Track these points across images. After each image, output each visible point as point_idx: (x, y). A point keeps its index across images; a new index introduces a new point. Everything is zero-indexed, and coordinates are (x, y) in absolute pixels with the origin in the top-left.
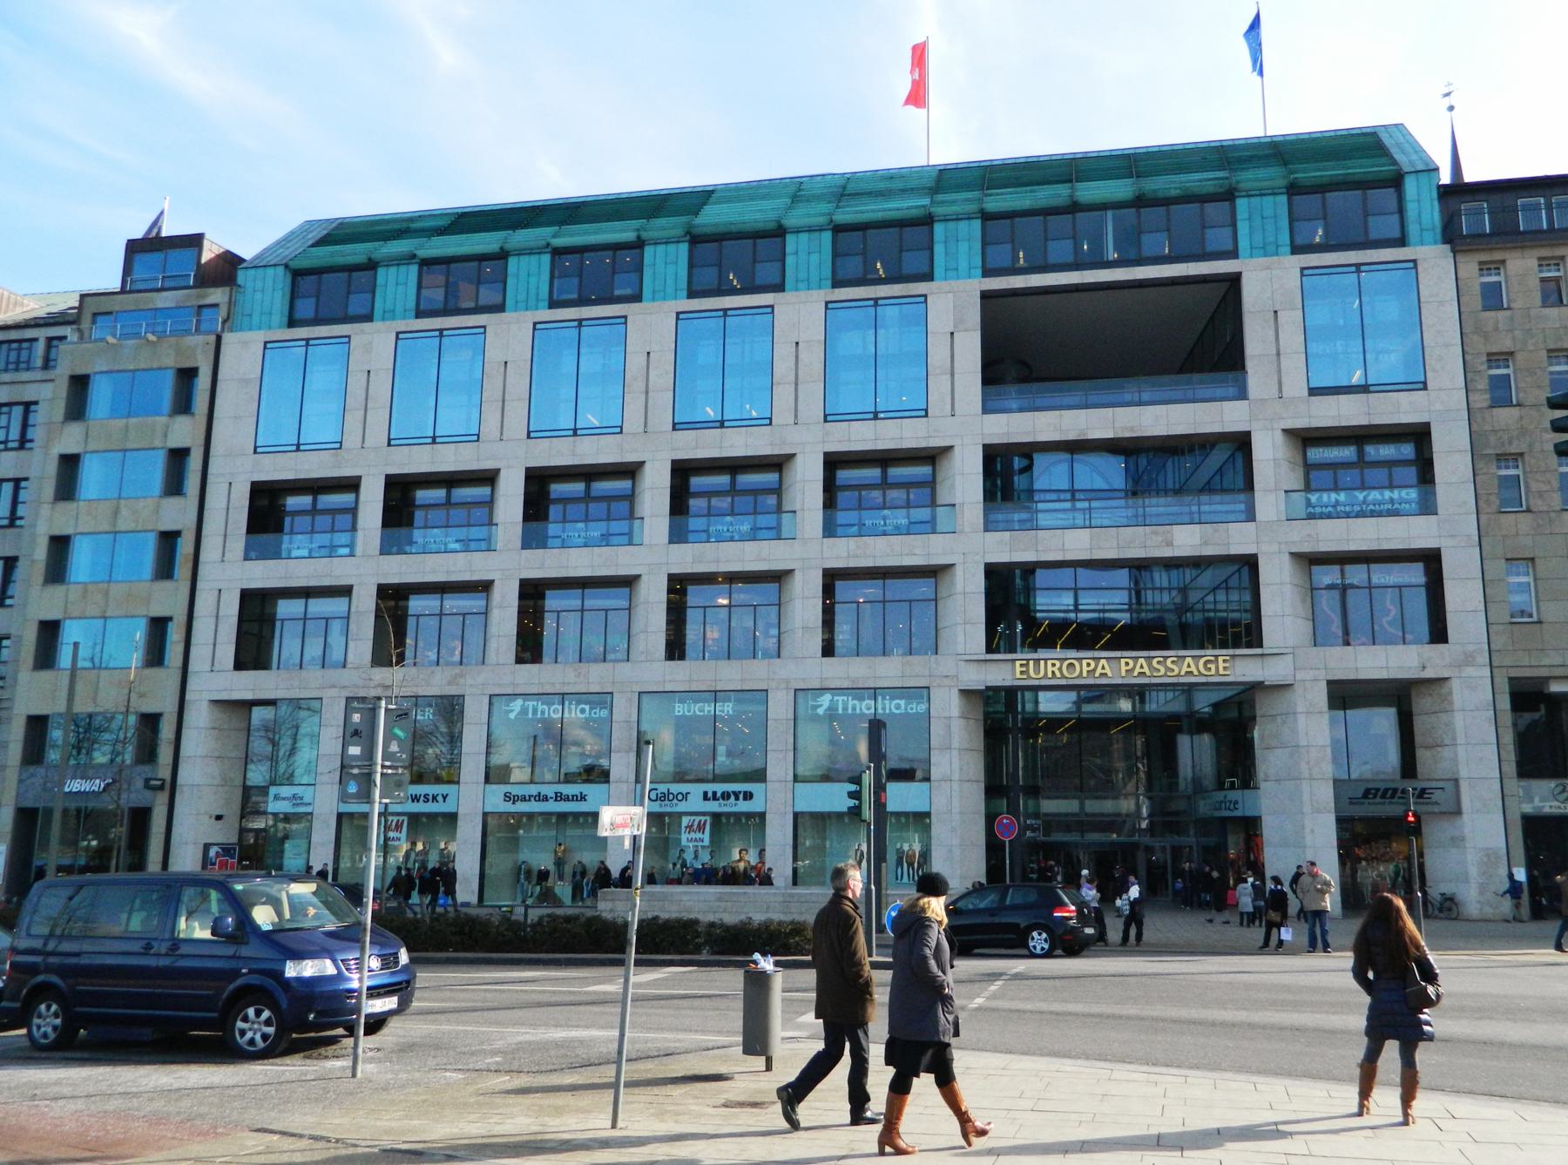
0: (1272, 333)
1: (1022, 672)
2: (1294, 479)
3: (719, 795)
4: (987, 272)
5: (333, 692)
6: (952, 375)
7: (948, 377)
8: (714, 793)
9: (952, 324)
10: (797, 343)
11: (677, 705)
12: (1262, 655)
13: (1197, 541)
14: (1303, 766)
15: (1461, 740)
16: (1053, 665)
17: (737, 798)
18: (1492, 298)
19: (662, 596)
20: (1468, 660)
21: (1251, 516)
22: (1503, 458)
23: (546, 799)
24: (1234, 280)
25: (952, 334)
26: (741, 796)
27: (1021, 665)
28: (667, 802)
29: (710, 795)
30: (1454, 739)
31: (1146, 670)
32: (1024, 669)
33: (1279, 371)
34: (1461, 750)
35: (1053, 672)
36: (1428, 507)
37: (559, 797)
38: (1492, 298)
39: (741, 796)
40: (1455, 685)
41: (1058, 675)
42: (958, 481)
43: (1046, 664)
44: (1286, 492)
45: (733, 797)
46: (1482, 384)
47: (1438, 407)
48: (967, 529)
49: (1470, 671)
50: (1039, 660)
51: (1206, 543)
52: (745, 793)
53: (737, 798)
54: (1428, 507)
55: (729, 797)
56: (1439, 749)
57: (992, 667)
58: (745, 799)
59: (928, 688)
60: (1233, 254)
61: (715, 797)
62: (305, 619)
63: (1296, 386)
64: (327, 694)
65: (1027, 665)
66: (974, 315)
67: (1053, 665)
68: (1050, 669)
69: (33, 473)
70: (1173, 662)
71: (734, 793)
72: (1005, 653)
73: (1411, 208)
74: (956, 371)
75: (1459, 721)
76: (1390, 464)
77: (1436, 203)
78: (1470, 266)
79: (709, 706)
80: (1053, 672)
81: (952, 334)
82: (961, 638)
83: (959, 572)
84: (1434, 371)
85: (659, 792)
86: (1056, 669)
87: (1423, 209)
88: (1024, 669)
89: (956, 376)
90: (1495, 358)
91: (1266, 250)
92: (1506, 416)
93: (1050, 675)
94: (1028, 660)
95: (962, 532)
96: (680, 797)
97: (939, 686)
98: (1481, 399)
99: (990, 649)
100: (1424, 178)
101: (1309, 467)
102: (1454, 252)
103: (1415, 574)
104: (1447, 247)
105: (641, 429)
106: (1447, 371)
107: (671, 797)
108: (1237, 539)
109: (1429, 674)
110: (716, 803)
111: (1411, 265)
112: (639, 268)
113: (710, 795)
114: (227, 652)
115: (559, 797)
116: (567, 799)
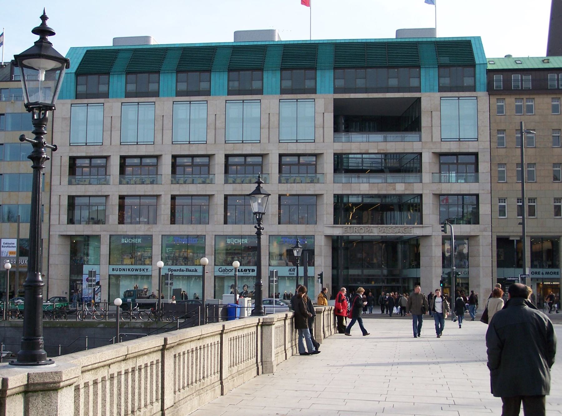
0: (430, 119)
1: (345, 231)
3: (243, 270)
4: (336, 91)
5: (105, 233)
6: (323, 128)
7: (322, 128)
8: (242, 270)
9: (323, 110)
10: (269, 114)
11: (228, 239)
12: (423, 227)
13: (403, 189)
14: (434, 263)
15: (481, 255)
16: (356, 229)
17: (249, 271)
18: (500, 110)
19: (223, 202)
20: (485, 230)
22: (500, 165)
23: (183, 271)
24: (419, 99)
25: (324, 113)
26: (251, 271)
27: (345, 229)
28: (225, 272)
29: (240, 270)
30: (479, 254)
31: (385, 231)
32: (346, 230)
33: (432, 132)
34: (481, 258)
35: (355, 231)
36: (477, 180)
37: (187, 270)
38: (500, 110)
39: (251, 271)
40: (480, 237)
41: (357, 232)
42: (325, 165)
43: (353, 229)
44: (432, 173)
45: (248, 271)
46: (495, 139)
47: (481, 147)
48: (328, 182)
49: (485, 233)
50: (351, 227)
51: (406, 190)
52: (252, 270)
53: (249, 271)
54: (477, 180)
55: (246, 271)
56: (475, 257)
57: (335, 229)
58: (252, 272)
59: (314, 235)
60: (418, 89)
61: (242, 271)
62: (89, 206)
63: (436, 138)
64: (102, 234)
65: (347, 228)
67: (356, 229)
68: (355, 230)
70: (394, 228)
71: (248, 269)
72: (340, 224)
73: (477, 76)
74: (325, 127)
75: (481, 249)
76: (466, 164)
77: (485, 75)
78: (494, 99)
79: (239, 240)
80: (355, 231)
81: (324, 113)
82: (325, 219)
83: (325, 197)
84: (481, 135)
85: (223, 269)
86: (356, 230)
87: (482, 78)
88: (346, 230)
89: (325, 129)
90: (499, 131)
92: (502, 151)
93: (354, 232)
94: (347, 227)
95: (326, 183)
96: (230, 271)
97: (318, 235)
98: (494, 145)
100: (482, 66)
101: (440, 164)
102: (489, 95)
103: (475, 197)
104: (487, 93)
105: (214, 142)
106: (485, 136)
107: (227, 271)
108: (417, 189)
109: (472, 234)
110: (243, 273)
111: (475, 98)
113: (240, 270)
115: (187, 270)
116: (190, 271)
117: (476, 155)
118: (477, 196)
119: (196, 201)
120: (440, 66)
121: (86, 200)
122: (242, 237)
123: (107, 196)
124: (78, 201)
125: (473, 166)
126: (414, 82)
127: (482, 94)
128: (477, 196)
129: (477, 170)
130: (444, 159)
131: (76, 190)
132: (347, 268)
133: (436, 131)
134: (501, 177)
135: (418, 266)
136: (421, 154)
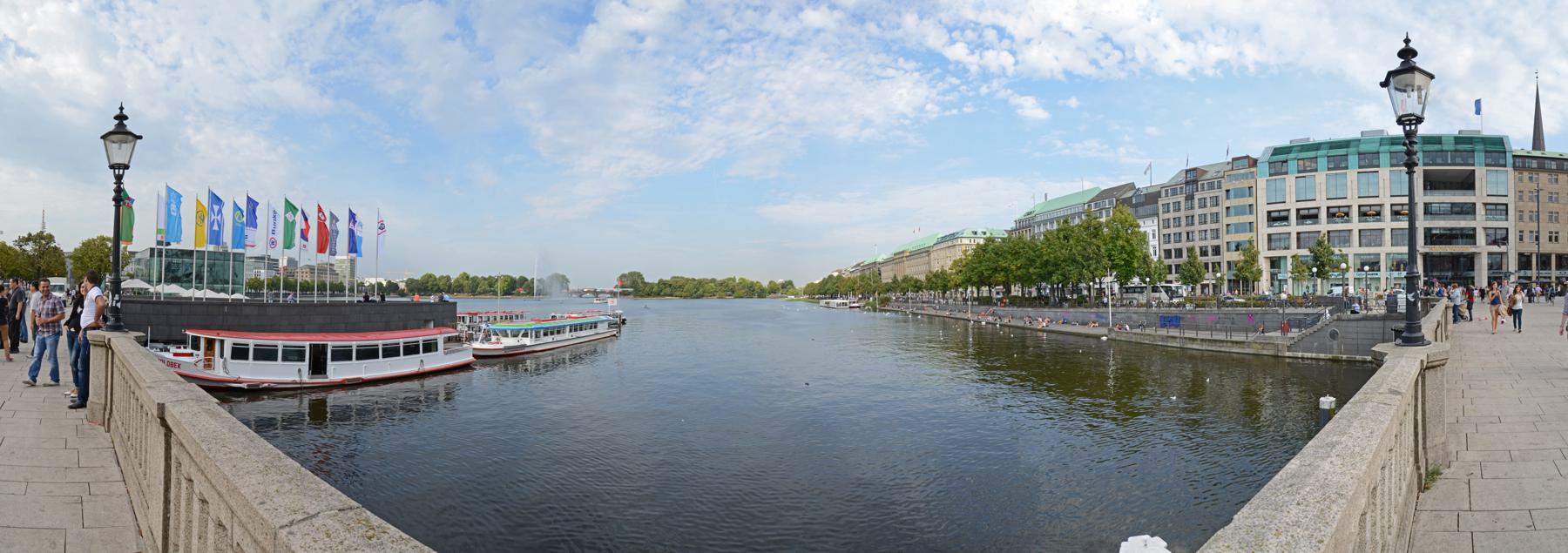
2: (1483, 212)
19: (1358, 233)
21: (1475, 219)
24: (1474, 170)
46: (1517, 197)
54: (1507, 220)
60: (1473, 165)
63: (1485, 194)
66: (1422, 173)
69: (1220, 211)
91: (1480, 165)
92: (1521, 203)
98: (1517, 200)
99: (1425, 244)
101: (1487, 210)
106: (1512, 194)
108: (1472, 224)
112: (1347, 161)
114: (1266, 247)
117: (1506, 205)
118: (1507, 229)
119: (1342, 234)
120: (1486, 152)
121: (1278, 236)
122: (1369, 254)
123: (1290, 233)
124: (1273, 237)
125: (1505, 212)
126: (1470, 161)
127: (1510, 169)
128: (1507, 229)
129: (1507, 214)
130: (1488, 207)
131: (1272, 230)
132: (1432, 272)
133: (1484, 189)
134: (1521, 218)
135: (1473, 270)
136: (1475, 204)
